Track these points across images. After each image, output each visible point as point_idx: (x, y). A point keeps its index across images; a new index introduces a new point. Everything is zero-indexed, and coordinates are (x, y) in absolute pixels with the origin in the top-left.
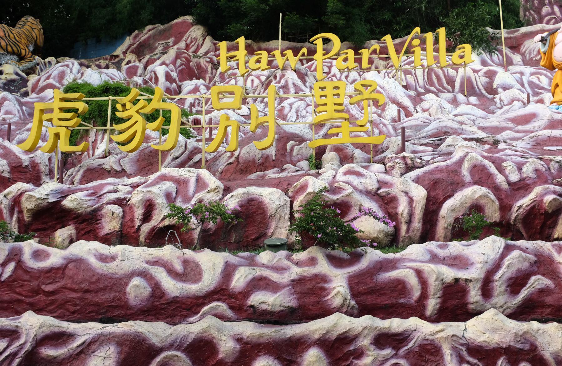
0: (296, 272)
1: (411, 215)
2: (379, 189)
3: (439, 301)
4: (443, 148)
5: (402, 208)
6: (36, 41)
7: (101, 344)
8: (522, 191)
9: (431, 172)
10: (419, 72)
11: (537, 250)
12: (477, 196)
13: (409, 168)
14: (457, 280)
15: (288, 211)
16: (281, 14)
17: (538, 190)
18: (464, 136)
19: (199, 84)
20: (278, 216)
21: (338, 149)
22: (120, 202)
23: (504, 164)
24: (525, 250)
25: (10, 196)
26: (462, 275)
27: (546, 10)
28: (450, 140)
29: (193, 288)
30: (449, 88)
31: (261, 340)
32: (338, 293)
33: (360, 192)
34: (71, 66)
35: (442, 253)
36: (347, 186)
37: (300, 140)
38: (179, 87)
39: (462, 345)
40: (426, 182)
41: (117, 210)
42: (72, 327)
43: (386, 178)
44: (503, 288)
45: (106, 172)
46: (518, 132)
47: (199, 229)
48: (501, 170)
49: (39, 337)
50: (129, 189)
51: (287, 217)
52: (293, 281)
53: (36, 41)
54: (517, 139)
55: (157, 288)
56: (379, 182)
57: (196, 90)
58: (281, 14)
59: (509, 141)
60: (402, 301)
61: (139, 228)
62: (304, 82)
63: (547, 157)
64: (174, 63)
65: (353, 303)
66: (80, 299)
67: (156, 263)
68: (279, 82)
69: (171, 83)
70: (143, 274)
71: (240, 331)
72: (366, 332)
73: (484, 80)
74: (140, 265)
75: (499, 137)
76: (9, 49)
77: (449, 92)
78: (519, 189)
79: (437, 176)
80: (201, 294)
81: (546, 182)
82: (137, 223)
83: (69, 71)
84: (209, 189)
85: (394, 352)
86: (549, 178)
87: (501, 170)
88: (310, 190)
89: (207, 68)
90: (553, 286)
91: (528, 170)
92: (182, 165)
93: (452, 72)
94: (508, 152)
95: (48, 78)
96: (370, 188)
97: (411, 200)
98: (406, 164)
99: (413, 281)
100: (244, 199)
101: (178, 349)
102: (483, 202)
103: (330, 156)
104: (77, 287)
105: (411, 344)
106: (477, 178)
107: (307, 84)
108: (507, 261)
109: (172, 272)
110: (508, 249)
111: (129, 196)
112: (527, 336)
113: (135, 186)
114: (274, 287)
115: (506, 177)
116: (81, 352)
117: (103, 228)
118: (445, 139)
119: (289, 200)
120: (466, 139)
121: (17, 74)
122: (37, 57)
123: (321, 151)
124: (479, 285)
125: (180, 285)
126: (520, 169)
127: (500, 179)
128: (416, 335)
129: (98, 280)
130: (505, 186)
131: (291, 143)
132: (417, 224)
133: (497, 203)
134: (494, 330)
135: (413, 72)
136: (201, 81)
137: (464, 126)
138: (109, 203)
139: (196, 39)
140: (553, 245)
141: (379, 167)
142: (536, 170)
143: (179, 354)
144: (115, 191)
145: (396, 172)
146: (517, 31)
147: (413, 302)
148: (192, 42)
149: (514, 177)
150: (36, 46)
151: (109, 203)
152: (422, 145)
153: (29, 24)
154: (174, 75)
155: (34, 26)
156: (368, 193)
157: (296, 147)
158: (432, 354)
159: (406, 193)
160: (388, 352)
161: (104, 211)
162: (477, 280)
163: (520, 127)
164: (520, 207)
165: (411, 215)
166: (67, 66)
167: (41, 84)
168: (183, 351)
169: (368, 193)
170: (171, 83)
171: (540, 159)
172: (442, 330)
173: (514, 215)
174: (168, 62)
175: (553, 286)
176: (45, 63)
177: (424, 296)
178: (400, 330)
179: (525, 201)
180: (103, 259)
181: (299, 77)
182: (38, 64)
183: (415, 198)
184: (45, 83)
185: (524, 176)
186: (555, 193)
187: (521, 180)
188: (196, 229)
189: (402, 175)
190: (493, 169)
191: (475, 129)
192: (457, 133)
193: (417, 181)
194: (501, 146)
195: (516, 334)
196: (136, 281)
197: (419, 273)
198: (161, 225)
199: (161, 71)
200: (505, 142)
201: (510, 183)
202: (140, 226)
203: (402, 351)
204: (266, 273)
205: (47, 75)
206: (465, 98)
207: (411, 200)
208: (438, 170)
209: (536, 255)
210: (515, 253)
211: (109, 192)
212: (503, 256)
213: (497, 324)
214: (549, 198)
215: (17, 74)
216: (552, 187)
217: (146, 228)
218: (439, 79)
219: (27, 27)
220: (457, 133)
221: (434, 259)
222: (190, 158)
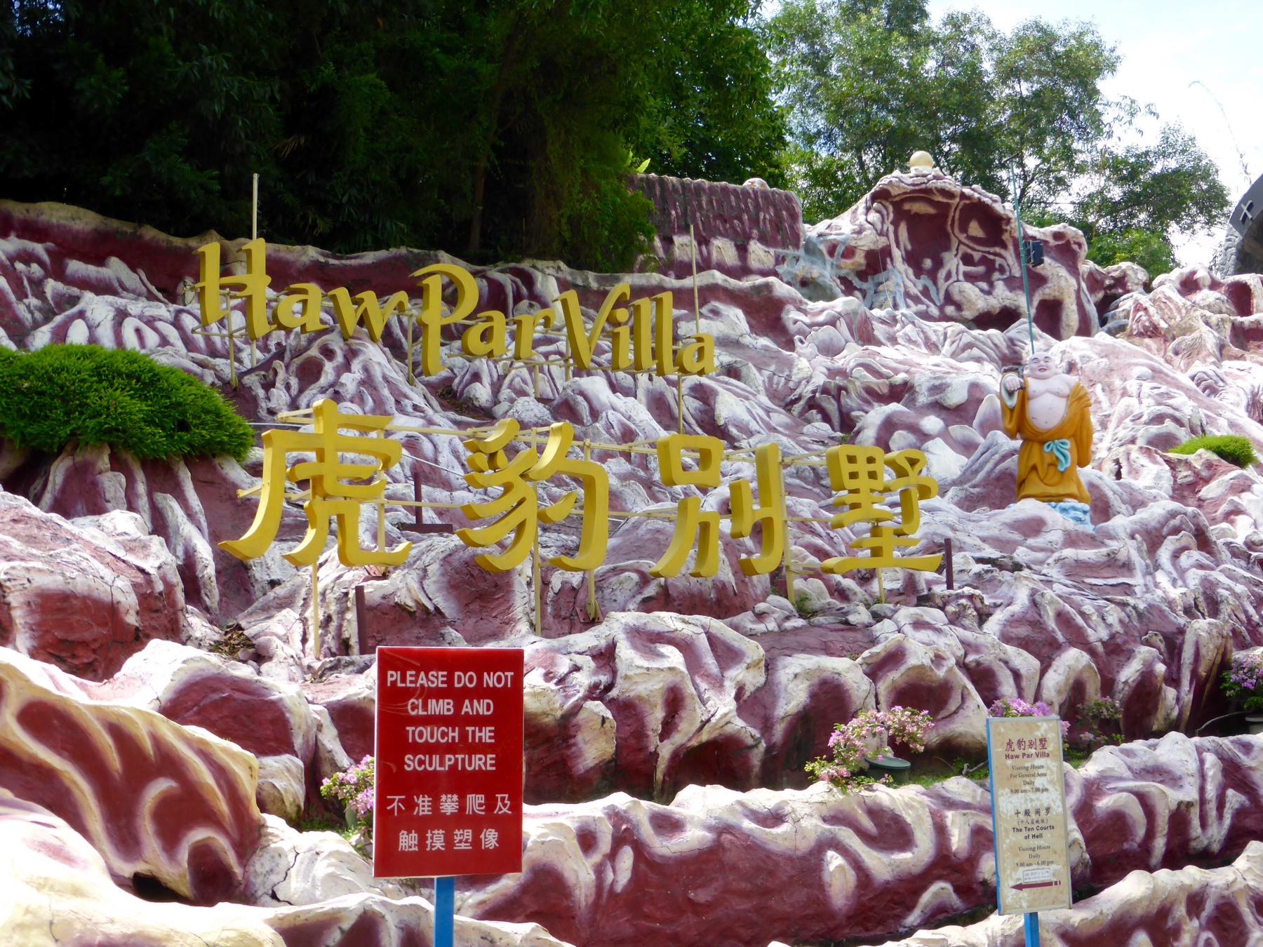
16: (256, 176)
45: (404, 614)
47: (763, 745)
58: (256, 176)
80: (917, 870)
84: (749, 661)
99: (1136, 812)
117: (579, 755)
135: (546, 367)
140: (1232, 742)
147: (1136, 845)
159: (1006, 663)
161: (582, 716)
183: (1023, 672)
188: (756, 746)
197: (1142, 797)
198: (694, 743)
200: (1029, 568)
217: (666, 750)
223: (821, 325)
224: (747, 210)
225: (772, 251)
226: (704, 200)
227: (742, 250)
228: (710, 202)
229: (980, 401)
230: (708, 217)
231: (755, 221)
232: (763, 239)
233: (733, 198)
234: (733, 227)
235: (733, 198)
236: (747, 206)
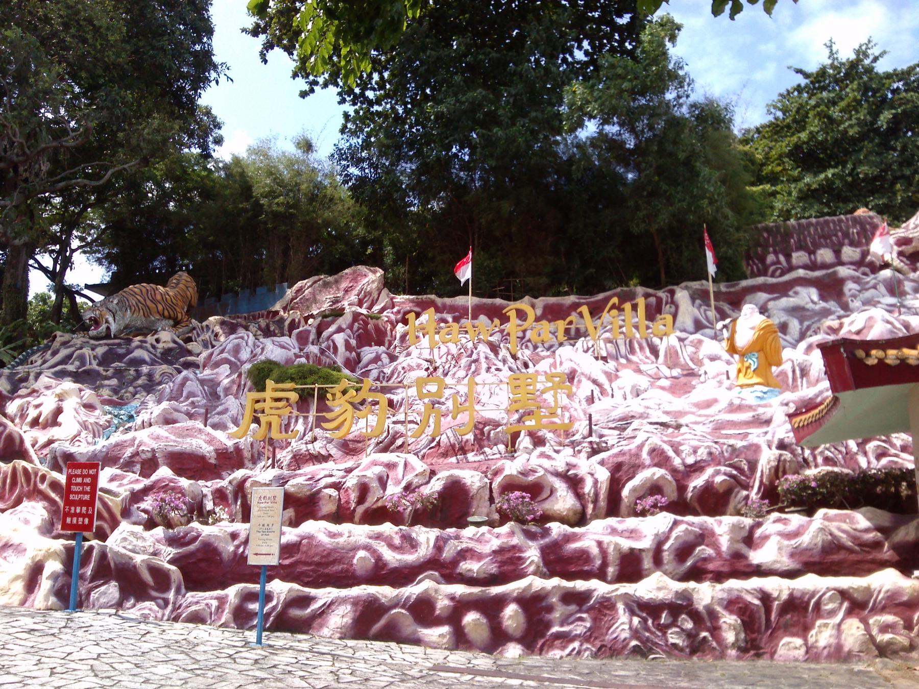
0: (495, 544)
1: (596, 495)
2: (568, 471)
3: (617, 568)
4: (629, 432)
5: (588, 488)
6: (190, 301)
7: (339, 605)
8: (697, 473)
9: (616, 455)
10: (621, 342)
11: (702, 525)
12: (655, 477)
13: (594, 452)
14: (632, 550)
15: (488, 492)
17: (709, 471)
18: (650, 421)
19: (380, 352)
20: (478, 496)
21: (531, 434)
22: (337, 486)
23: (681, 448)
24: (692, 524)
25: (234, 483)
26: (637, 545)
27: (771, 258)
28: (635, 424)
29: (410, 558)
30: (653, 358)
31: (470, 598)
32: (532, 562)
33: (552, 474)
34: (246, 338)
35: (620, 527)
36: (540, 469)
37: (497, 424)
38: (358, 355)
39: (634, 601)
40: (610, 465)
41: (333, 492)
42: (313, 592)
43: (573, 460)
44: (672, 557)
46: (700, 416)
48: (677, 452)
49: (288, 600)
50: (342, 473)
51: (487, 497)
52: (494, 552)
53: (190, 301)
54: (696, 423)
55: (379, 559)
56: (567, 464)
57: (377, 359)
59: (690, 425)
60: (586, 568)
61: (354, 510)
62: (496, 353)
63: (722, 441)
64: (351, 327)
65: (545, 570)
66: (312, 570)
67: (378, 537)
68: (470, 356)
69: (351, 352)
70: (367, 548)
71: (453, 592)
72: (555, 590)
73: (690, 349)
74: (363, 540)
75: (682, 421)
76: (166, 313)
77: (653, 362)
78: (695, 471)
79: (620, 459)
81: (719, 464)
82: (353, 505)
83: (244, 344)
84: (417, 472)
85: (578, 608)
86: (722, 460)
87: (677, 452)
88: (507, 472)
89: (386, 329)
90: (714, 555)
91: (702, 454)
92: (385, 450)
93: (656, 341)
94: (687, 436)
95: (222, 352)
96: (560, 470)
97: (596, 482)
98: (592, 448)
99: (595, 551)
100: (449, 481)
101: (403, 607)
102: (661, 483)
103: (525, 441)
104: (310, 561)
105: (592, 602)
106: (656, 461)
107: (500, 357)
108: (674, 535)
109: (392, 546)
110: (676, 523)
111: (344, 480)
112: (686, 594)
113: (349, 471)
114: (479, 557)
115: (683, 460)
116: (323, 612)
117: (320, 509)
118: (630, 423)
119: (488, 481)
120: (651, 423)
121: (175, 342)
122: (193, 321)
123: (515, 436)
124: (651, 554)
125: (399, 557)
126: (695, 452)
127: (677, 462)
128: (596, 594)
129: (329, 554)
130: (681, 468)
131: (487, 428)
132: (602, 503)
133: (674, 483)
134: (659, 589)
136: (382, 348)
137: (649, 411)
138: (325, 487)
139: (370, 293)
141: (569, 451)
142: (710, 454)
143: (403, 611)
144: (331, 476)
145: (583, 455)
146: (737, 284)
148: (365, 296)
149: (690, 460)
150: (190, 307)
151: (325, 487)
152: (610, 428)
153: (183, 282)
154: (353, 342)
155: (189, 284)
156: (557, 474)
157: (492, 432)
158: (609, 609)
159: (592, 475)
160: (573, 608)
161: (322, 494)
162: (648, 550)
163: (703, 412)
164: (695, 487)
165: (596, 495)
166: (242, 338)
167: (215, 358)
168: (407, 610)
169: (557, 474)
170: (351, 352)
171: (716, 443)
172: (617, 589)
173: (690, 495)
174: (344, 326)
175: (714, 555)
176: (202, 327)
177: (605, 565)
178: (583, 589)
179: (697, 482)
180: (332, 535)
181: (491, 350)
182: (194, 329)
184: (219, 357)
185: (699, 459)
186: (725, 474)
187: (696, 462)
189: (588, 458)
190: (671, 453)
191: (660, 413)
192: (642, 416)
193: (602, 463)
194: (683, 430)
195: (677, 592)
196: (361, 554)
197: (600, 544)
198: (375, 506)
199: (339, 339)
200: (687, 426)
201: (686, 466)
202: (355, 508)
203: (585, 607)
204: (471, 545)
205: (221, 348)
206: (668, 370)
207: (596, 482)
208: (622, 453)
209: (700, 529)
210: (682, 527)
211: (325, 476)
212: (671, 529)
213: (661, 584)
214: (719, 479)
215: (175, 342)
216: (723, 469)
217: (361, 509)
218: (641, 348)
219: (181, 285)
220: (642, 416)
221: (614, 531)
222: (392, 442)
223: (867, 290)
224: (841, 230)
225: (858, 250)
226: (812, 230)
227: (837, 253)
228: (816, 230)
229: (871, 327)
230: (814, 239)
231: (846, 235)
232: (852, 244)
233: (831, 225)
234: (832, 241)
235: (831, 225)
236: (841, 227)
